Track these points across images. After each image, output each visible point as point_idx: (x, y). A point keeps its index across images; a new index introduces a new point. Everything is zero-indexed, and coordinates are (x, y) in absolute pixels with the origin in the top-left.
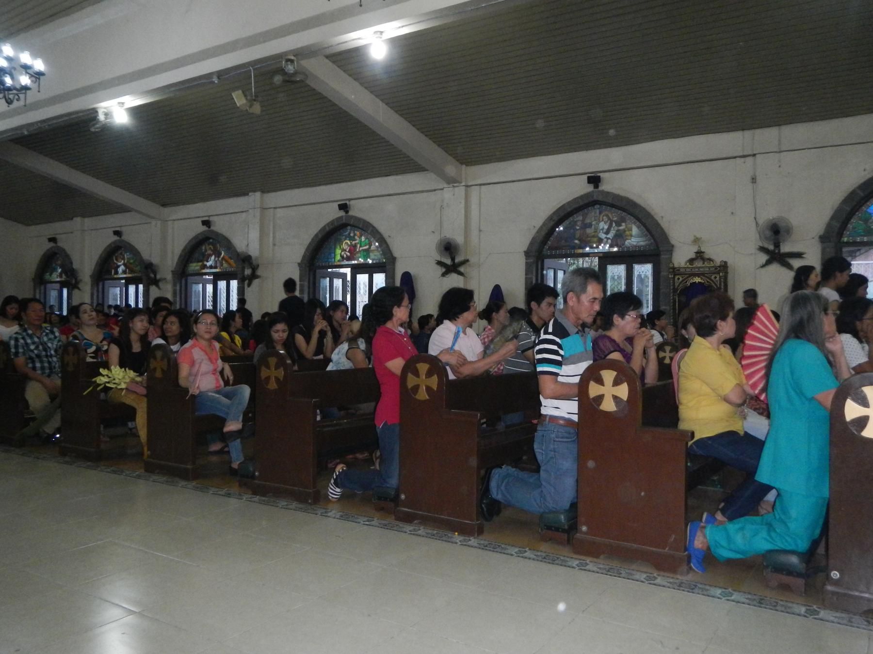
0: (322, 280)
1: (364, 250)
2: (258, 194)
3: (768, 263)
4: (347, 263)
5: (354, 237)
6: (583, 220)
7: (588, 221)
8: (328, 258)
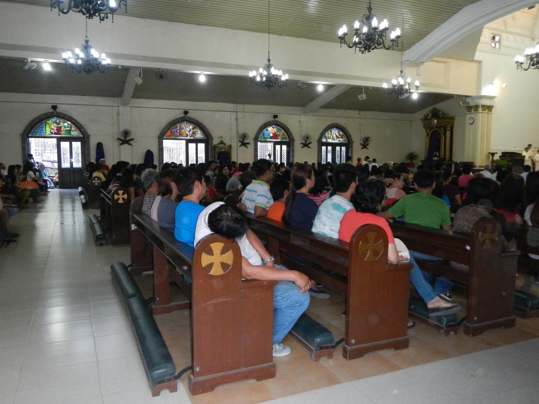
6: (180, 127)
7: (182, 127)
8: (41, 133)
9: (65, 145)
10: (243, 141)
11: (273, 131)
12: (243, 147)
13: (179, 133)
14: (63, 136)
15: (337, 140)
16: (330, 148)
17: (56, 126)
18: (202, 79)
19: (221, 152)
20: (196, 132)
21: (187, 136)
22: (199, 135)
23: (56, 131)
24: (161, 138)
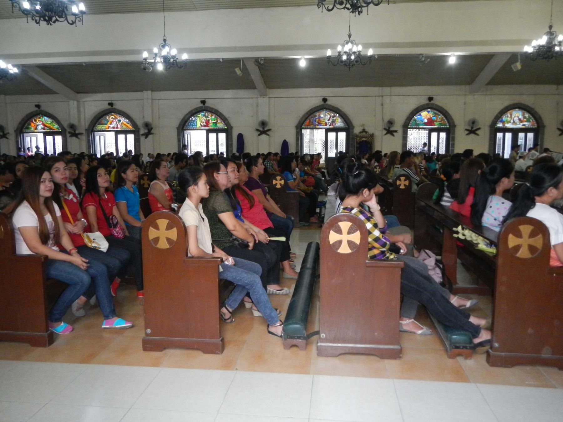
0: (27, 138)
1: (214, 123)
2: (149, 92)
3: (386, 134)
4: (203, 128)
5: (208, 116)
8: (193, 126)
9: (213, 136)
10: (389, 128)
11: (428, 117)
12: (389, 135)
13: (318, 122)
14: (211, 128)
15: (520, 124)
16: (509, 136)
17: (205, 119)
18: (303, 64)
19: (361, 141)
20: (335, 120)
21: (326, 125)
22: (339, 123)
23: (205, 124)
24: (299, 128)
